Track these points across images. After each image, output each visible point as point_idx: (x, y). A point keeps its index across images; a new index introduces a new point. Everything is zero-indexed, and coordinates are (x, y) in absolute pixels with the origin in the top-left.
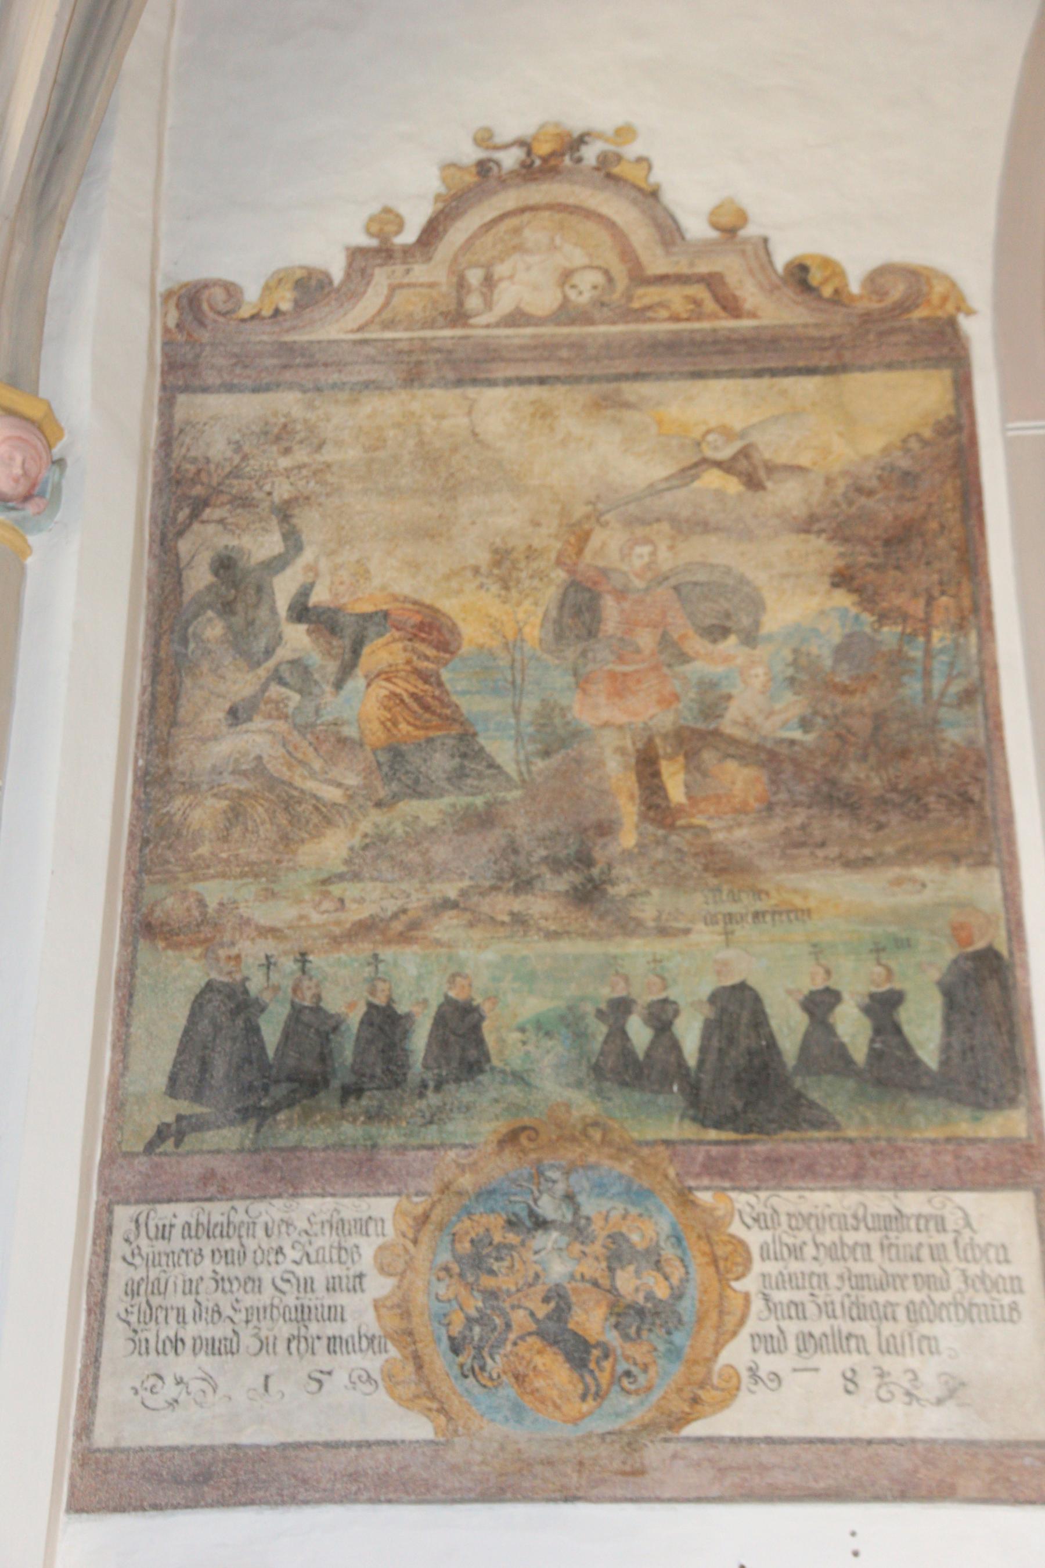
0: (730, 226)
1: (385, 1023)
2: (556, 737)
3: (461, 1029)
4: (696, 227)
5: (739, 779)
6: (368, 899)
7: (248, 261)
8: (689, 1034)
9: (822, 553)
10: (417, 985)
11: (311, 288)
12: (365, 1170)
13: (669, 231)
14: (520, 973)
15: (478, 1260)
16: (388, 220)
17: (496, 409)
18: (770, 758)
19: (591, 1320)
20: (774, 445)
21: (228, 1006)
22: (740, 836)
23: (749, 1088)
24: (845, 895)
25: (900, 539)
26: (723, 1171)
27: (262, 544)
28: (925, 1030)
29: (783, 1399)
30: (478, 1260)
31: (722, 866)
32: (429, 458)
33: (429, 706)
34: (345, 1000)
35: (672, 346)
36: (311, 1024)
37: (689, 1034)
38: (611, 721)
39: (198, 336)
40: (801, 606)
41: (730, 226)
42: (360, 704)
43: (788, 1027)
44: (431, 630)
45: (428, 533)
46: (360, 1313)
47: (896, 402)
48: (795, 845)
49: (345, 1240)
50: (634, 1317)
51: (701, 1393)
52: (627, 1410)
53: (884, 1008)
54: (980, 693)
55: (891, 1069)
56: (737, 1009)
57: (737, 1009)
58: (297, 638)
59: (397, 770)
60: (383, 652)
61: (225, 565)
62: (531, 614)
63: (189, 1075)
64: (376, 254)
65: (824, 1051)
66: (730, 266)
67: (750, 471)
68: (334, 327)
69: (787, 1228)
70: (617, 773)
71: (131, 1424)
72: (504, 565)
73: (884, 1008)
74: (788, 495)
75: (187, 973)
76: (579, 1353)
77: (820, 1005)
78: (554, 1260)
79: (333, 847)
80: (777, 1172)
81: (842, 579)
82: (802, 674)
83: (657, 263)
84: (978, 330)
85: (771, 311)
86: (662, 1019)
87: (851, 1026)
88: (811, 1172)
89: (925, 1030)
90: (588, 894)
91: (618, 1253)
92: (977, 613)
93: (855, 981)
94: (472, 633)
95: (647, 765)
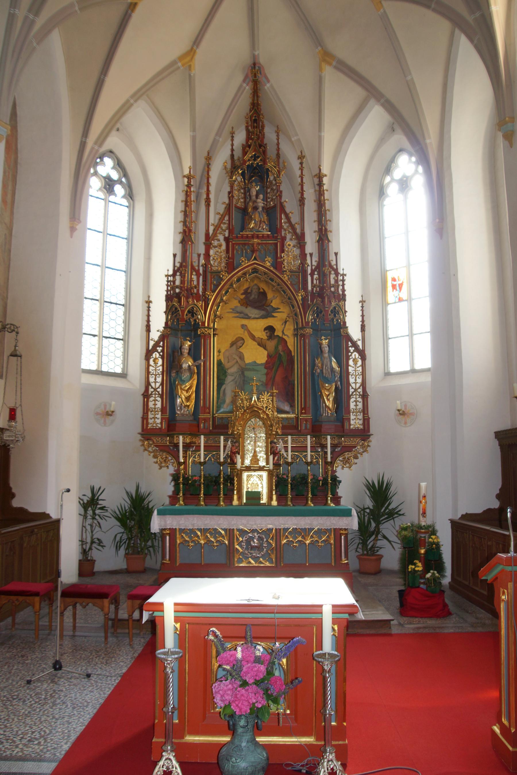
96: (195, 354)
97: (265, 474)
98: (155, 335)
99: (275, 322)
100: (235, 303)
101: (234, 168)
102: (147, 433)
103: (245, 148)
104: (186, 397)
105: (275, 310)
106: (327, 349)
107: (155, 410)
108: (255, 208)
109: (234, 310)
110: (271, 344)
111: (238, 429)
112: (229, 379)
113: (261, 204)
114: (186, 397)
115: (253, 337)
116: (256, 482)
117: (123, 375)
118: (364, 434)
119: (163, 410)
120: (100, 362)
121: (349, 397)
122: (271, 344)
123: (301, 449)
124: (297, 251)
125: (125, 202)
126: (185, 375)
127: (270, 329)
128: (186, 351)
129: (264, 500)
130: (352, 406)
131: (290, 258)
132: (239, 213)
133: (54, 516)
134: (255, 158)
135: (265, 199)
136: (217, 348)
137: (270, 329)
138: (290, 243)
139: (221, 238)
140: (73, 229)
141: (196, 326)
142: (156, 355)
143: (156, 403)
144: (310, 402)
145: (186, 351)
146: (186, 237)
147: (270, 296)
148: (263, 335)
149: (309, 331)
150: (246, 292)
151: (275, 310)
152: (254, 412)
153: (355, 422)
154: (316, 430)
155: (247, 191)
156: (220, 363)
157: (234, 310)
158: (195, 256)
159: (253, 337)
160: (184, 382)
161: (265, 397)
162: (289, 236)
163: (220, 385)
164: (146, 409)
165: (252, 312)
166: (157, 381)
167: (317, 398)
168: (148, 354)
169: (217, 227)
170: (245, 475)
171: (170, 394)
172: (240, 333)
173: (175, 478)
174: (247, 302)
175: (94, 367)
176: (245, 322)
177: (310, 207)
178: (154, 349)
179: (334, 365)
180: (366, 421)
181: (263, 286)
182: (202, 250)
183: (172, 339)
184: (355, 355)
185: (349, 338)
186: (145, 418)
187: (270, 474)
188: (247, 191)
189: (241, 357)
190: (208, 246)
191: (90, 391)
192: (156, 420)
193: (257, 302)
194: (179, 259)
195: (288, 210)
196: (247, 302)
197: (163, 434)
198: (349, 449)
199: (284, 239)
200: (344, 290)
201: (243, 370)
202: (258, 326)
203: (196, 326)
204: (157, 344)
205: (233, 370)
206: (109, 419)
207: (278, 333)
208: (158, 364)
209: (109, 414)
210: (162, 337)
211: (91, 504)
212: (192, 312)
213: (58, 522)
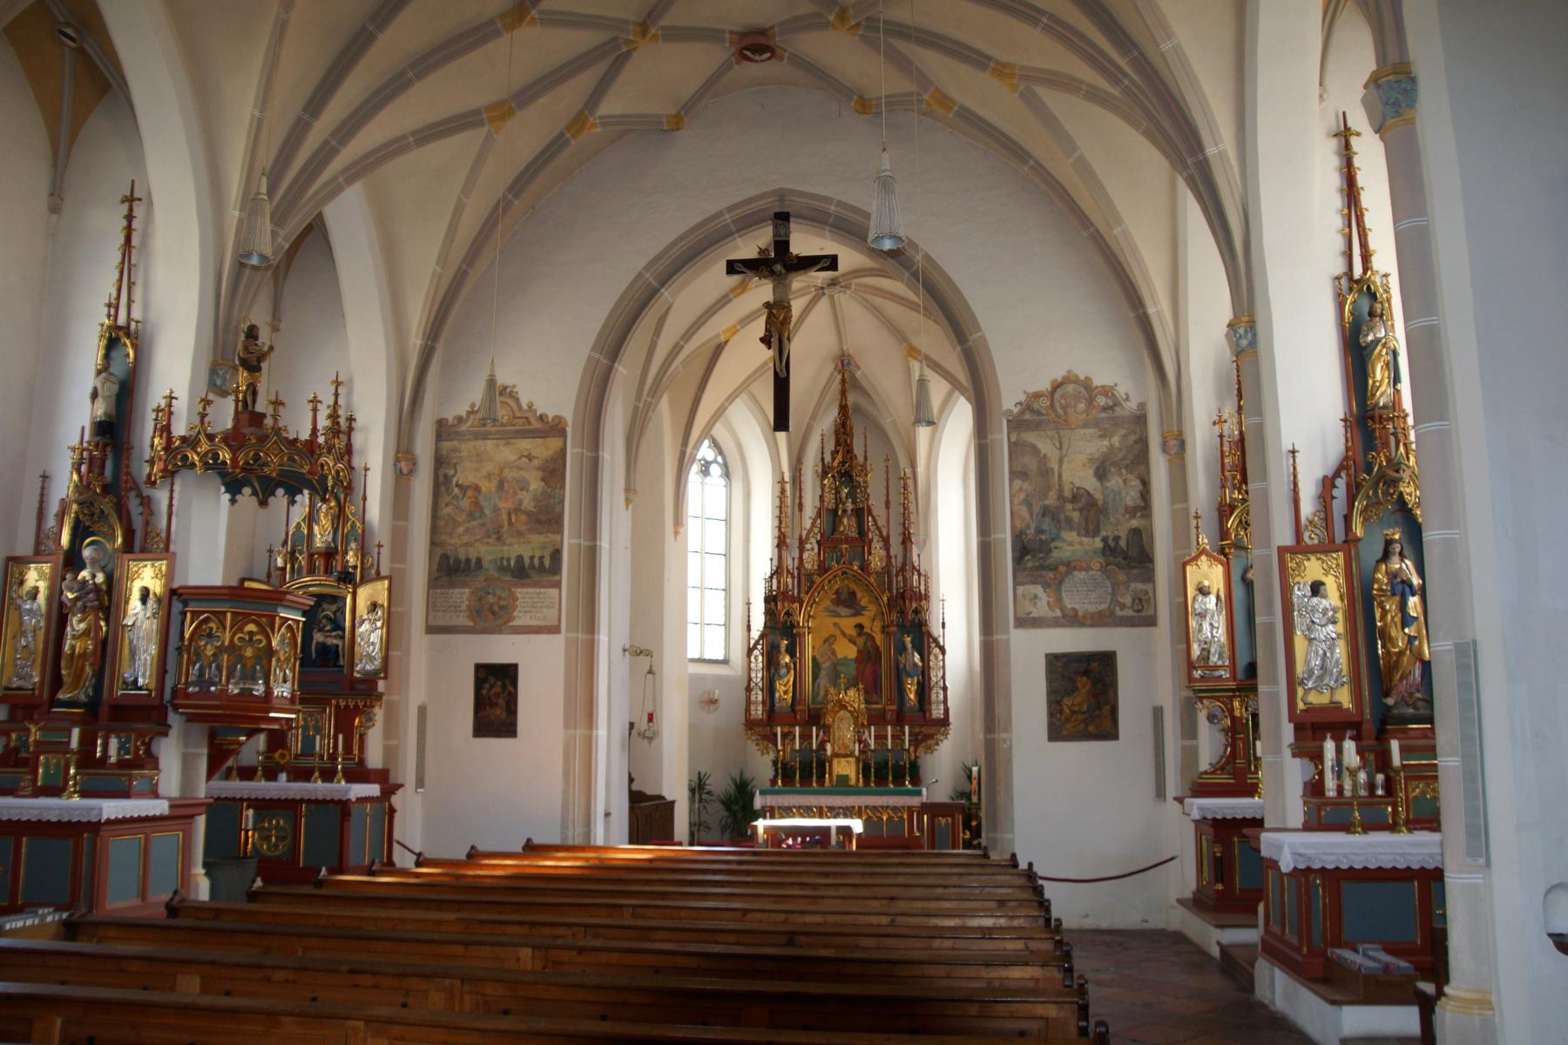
0: (530, 406)
1: (468, 560)
2: (496, 510)
3: (479, 561)
4: (525, 407)
5: (523, 518)
6: (466, 539)
7: (450, 415)
8: (512, 563)
9: (540, 474)
10: (473, 554)
11: (460, 419)
12: (464, 585)
13: (520, 407)
14: (487, 552)
15: (480, 599)
16: (473, 405)
17: (489, 444)
18: (528, 513)
19: (496, 608)
20: (534, 453)
21: (445, 557)
22: (523, 528)
23: (521, 572)
24: (537, 539)
25: (553, 471)
26: (516, 585)
27: (452, 472)
28: (547, 562)
29: (521, 620)
30: (480, 599)
31: (520, 534)
32: (478, 455)
33: (476, 503)
34: (462, 557)
35: (518, 432)
36: (457, 561)
37: (512, 563)
38: (505, 506)
39: (443, 430)
40: (536, 485)
41: (530, 406)
42: (465, 503)
43: (527, 561)
44: (477, 489)
45: (477, 470)
46: (464, 607)
47: (555, 443)
48: (531, 530)
49: (462, 595)
50: (502, 608)
51: (511, 618)
52: (499, 622)
53: (541, 558)
54: (562, 502)
55: (541, 569)
56: (520, 558)
57: (520, 558)
58: (456, 490)
59: (471, 516)
60: (470, 493)
61: (445, 476)
62: (493, 485)
63: (440, 569)
64: (469, 413)
65: (532, 566)
66: (529, 415)
67: (530, 457)
68: (464, 428)
69: (524, 594)
70: (505, 516)
71: (433, 622)
72: (489, 476)
73: (541, 558)
74: (536, 462)
75: (439, 551)
76: (494, 613)
77: (532, 558)
78: (491, 599)
79: (461, 530)
80: (523, 586)
81: (543, 480)
82: (535, 499)
83: (518, 414)
84: (569, 430)
85: (536, 424)
86: (509, 560)
87: (536, 562)
88: (529, 586)
89: (547, 562)
90: (499, 539)
91: (500, 598)
92: (563, 487)
93: (538, 554)
94: (484, 490)
95: (509, 515)
96: (791, 651)
97: (852, 760)
98: (755, 634)
99: (864, 620)
100: (827, 603)
101: (824, 474)
102: (750, 724)
103: (835, 453)
104: (784, 689)
105: (864, 608)
106: (909, 646)
107: (756, 703)
108: (845, 511)
109: (827, 609)
110: (860, 641)
111: (829, 720)
112: (823, 673)
113: (849, 506)
114: (784, 689)
115: (844, 634)
116: (845, 768)
117: (725, 662)
118: (944, 722)
119: (764, 702)
120: (702, 651)
121: (930, 689)
122: (860, 641)
123: (880, 737)
124: (883, 553)
125: (722, 482)
126: (783, 671)
127: (860, 627)
128: (783, 649)
129: (853, 782)
130: (933, 697)
131: (876, 560)
132: (831, 516)
133: (669, 798)
134: (843, 463)
135: (854, 502)
136: (809, 645)
137: (860, 627)
138: (877, 546)
139: (813, 541)
140: (676, 533)
141: (792, 626)
142: (756, 652)
143: (758, 696)
144: (895, 694)
145: (783, 649)
146: (781, 543)
147: (859, 595)
148: (854, 633)
149: (894, 629)
150: (837, 592)
151: (864, 608)
152: (842, 706)
153: (937, 712)
154: (899, 720)
155: (838, 492)
156: (814, 659)
157: (827, 609)
158: (790, 562)
159: (844, 634)
160: (781, 677)
161: (851, 692)
162: (876, 539)
163: (814, 679)
164: (749, 702)
165: (844, 611)
166: (758, 676)
167: (901, 691)
168: (750, 651)
169: (810, 531)
170: (835, 761)
171: (770, 689)
172: (833, 630)
173: (775, 763)
174: (839, 601)
175: (697, 656)
176: (836, 620)
177: (896, 509)
178: (755, 647)
179: (917, 657)
180: (947, 711)
181: (853, 586)
182: (797, 555)
183: (771, 638)
184: (937, 650)
185: (930, 635)
186: (748, 710)
187: (858, 760)
188: (838, 492)
189: (834, 653)
190: (802, 550)
191: (696, 680)
192: (758, 712)
193: (847, 601)
194: (775, 562)
195: (875, 512)
196: (839, 601)
197: (765, 724)
198: (931, 736)
199: (871, 541)
200: (926, 589)
201: (835, 666)
202: (848, 624)
203: (792, 626)
204: (757, 643)
205: (826, 665)
206: (712, 707)
207: (867, 630)
208: (758, 661)
209: (713, 702)
210: (762, 636)
211: (698, 788)
212: (788, 614)
213: (673, 803)
